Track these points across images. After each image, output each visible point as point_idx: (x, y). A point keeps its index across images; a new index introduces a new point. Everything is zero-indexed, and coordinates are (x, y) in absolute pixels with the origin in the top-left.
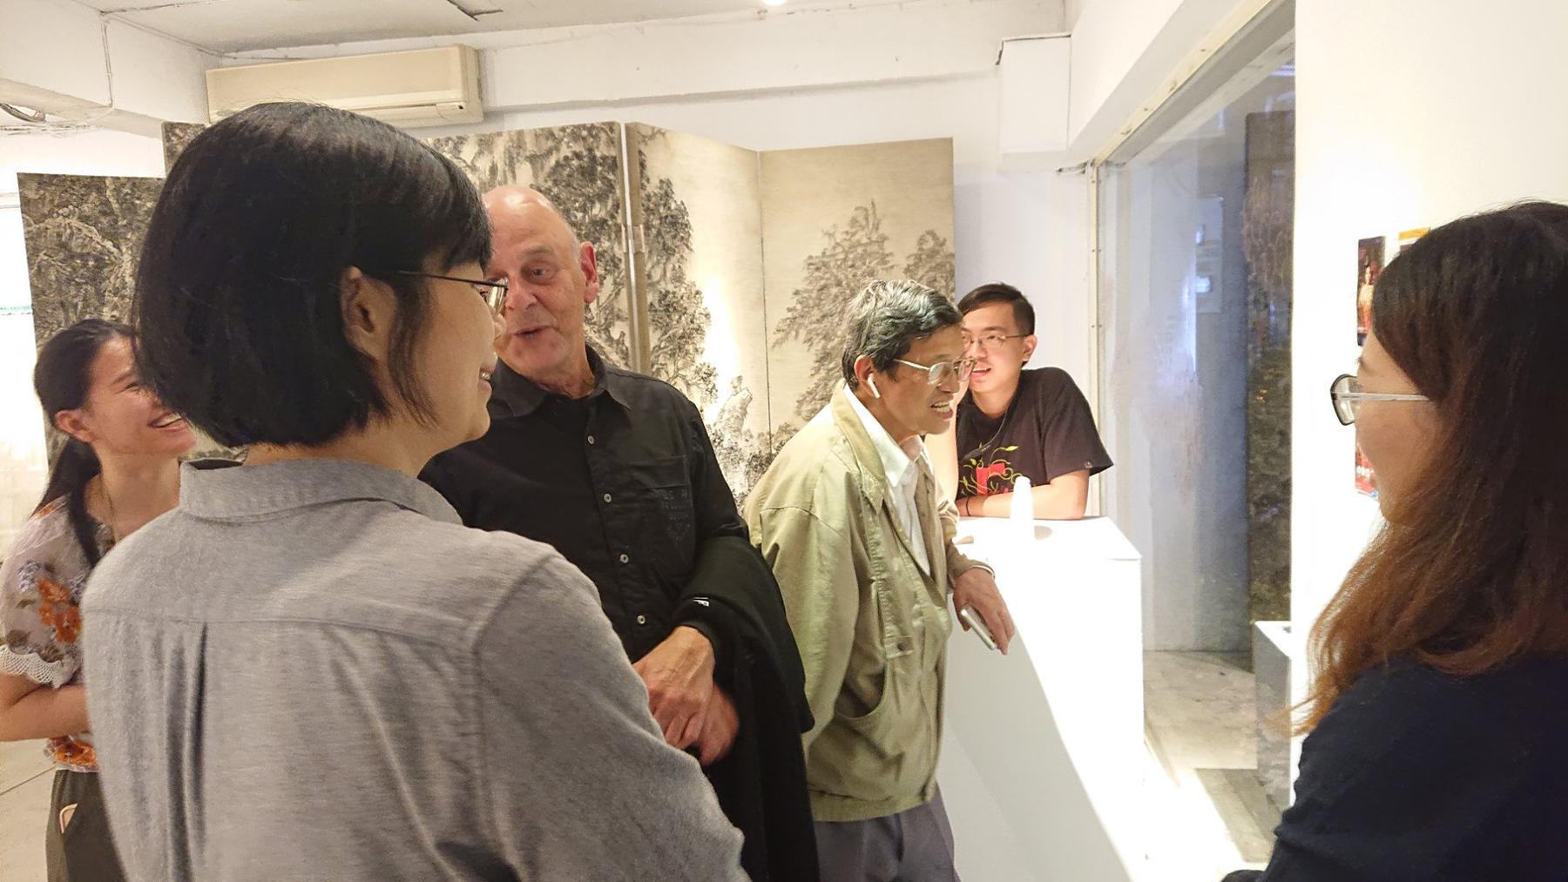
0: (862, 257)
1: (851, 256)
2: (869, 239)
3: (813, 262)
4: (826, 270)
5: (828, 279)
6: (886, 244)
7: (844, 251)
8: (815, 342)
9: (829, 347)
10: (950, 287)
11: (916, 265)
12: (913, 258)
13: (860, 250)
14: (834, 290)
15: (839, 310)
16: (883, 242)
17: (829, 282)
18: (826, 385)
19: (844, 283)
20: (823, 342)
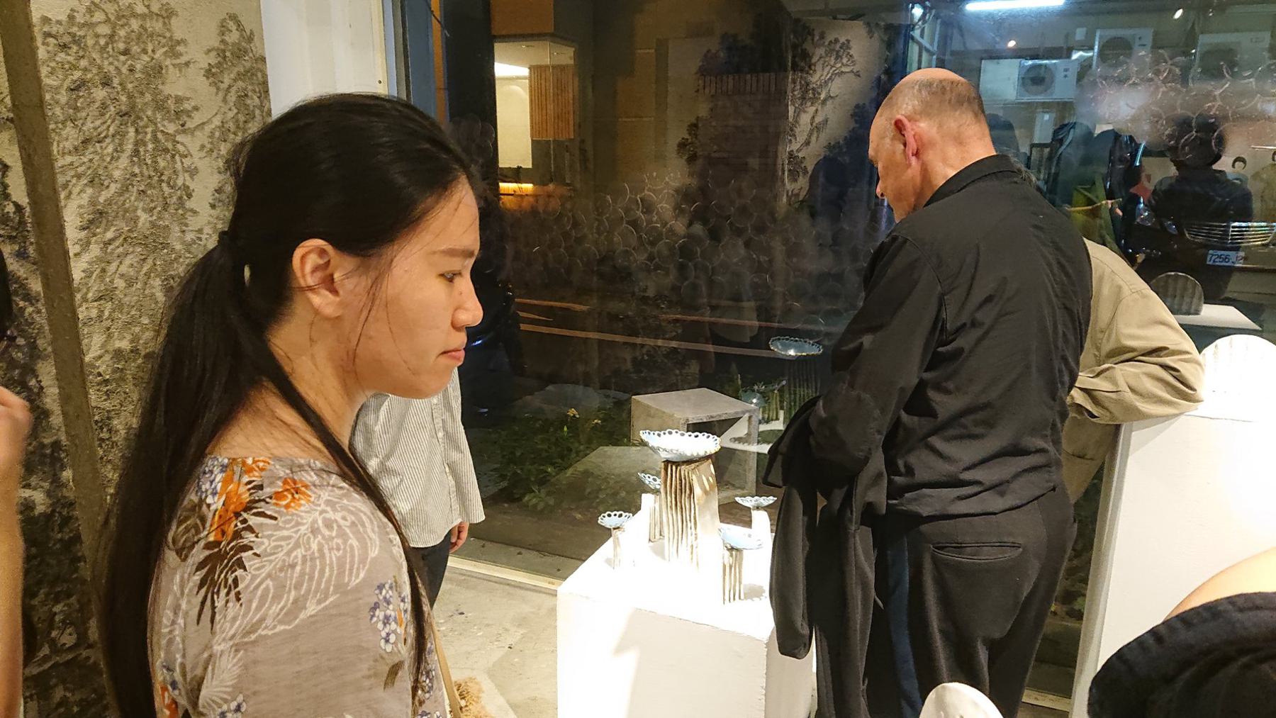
0: (142, 36)
1: (122, 33)
2: (148, 7)
3: (54, 30)
4: (81, 53)
5: (85, 70)
6: (173, 20)
7: (108, 21)
8: (76, 190)
9: (101, 200)
10: (266, 109)
11: (219, 65)
12: (213, 54)
13: (135, 24)
14: (100, 94)
15: (112, 130)
16: (169, 17)
17: (89, 76)
18: (104, 270)
19: (116, 81)
20: (89, 191)
